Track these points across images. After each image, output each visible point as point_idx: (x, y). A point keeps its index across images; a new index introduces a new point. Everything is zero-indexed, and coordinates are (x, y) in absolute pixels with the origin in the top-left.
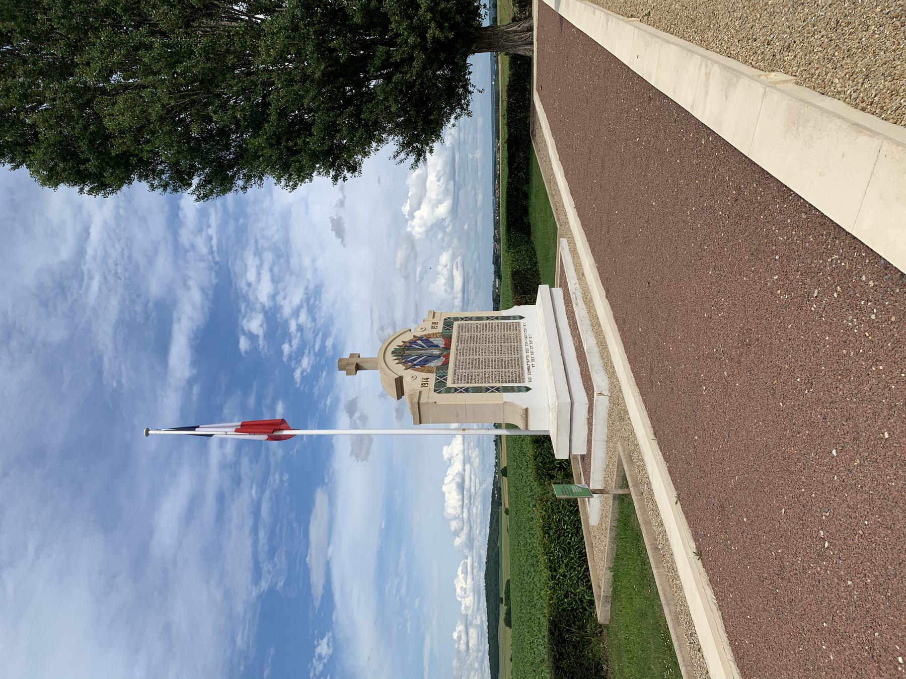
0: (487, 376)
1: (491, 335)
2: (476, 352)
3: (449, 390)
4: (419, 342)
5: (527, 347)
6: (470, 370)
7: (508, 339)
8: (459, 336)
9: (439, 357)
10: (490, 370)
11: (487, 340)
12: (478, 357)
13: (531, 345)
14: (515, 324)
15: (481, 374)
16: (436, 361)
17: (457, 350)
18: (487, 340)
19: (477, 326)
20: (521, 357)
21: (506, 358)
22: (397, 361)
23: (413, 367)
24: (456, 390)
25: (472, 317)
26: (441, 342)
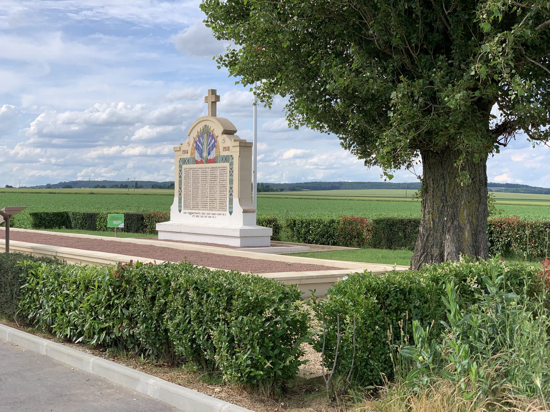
0: (188, 188)
1: (216, 190)
2: (204, 181)
3: (180, 166)
4: (213, 141)
5: (206, 214)
6: (192, 178)
7: (213, 202)
8: (216, 168)
9: (201, 156)
10: (191, 190)
11: (212, 188)
12: (200, 182)
13: (208, 217)
14: (225, 207)
15: (189, 184)
16: (199, 156)
17: (206, 168)
18: (212, 188)
19: (224, 180)
20: (199, 209)
21: (199, 199)
22: (199, 131)
23: (196, 142)
24: (180, 171)
25: (232, 176)
26: (211, 157)
